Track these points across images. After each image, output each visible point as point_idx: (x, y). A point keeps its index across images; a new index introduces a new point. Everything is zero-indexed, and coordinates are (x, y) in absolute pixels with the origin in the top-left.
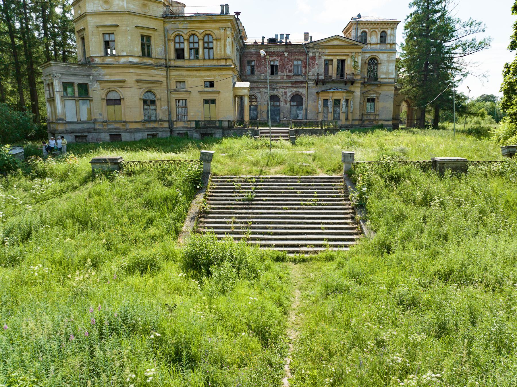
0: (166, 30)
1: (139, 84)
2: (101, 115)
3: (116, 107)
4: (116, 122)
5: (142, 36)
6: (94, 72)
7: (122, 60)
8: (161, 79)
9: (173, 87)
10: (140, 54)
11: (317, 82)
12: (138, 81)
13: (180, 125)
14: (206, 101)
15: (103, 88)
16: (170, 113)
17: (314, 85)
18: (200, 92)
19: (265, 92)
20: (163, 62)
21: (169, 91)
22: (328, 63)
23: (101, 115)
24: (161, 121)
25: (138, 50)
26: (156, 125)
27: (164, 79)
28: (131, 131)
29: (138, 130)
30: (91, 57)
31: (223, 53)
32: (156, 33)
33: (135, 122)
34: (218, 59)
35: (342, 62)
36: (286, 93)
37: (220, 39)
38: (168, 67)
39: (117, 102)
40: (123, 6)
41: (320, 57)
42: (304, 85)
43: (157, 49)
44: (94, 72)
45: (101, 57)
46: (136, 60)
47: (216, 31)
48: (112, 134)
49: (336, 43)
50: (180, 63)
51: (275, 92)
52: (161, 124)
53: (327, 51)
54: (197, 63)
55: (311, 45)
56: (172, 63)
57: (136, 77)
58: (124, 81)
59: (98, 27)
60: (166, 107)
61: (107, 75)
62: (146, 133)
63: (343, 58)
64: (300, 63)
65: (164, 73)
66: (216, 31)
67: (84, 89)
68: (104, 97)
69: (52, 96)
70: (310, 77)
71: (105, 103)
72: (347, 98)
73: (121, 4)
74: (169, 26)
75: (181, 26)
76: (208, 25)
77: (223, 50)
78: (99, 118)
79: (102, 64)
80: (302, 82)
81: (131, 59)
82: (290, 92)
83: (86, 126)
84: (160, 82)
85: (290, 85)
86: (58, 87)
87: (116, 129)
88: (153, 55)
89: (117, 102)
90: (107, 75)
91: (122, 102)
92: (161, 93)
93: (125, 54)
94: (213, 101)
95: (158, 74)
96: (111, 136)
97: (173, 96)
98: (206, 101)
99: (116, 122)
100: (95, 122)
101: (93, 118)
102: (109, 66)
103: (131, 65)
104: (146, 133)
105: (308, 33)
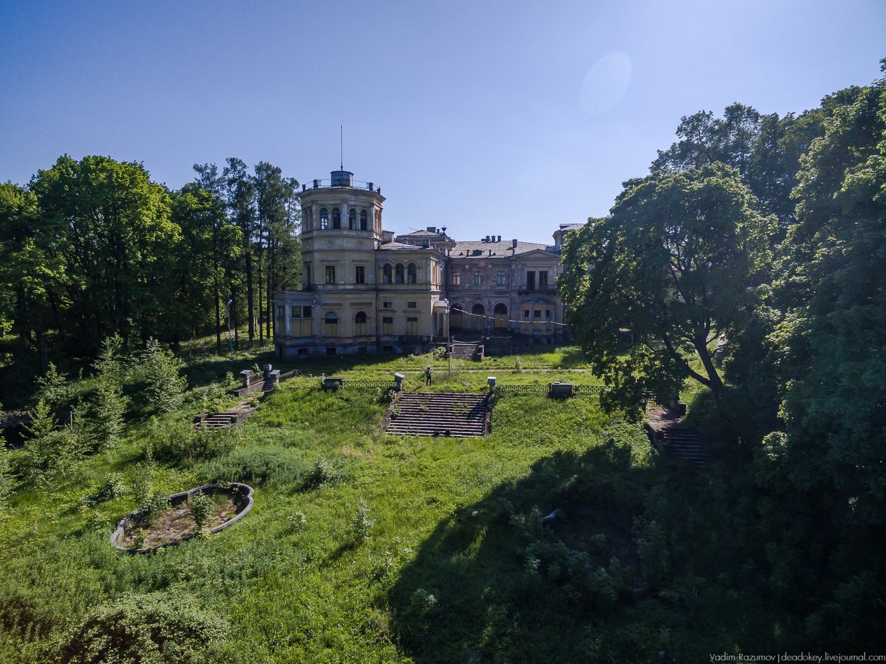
0: (377, 260)
1: (354, 307)
2: (320, 331)
3: (333, 324)
4: (332, 338)
5: (357, 268)
6: (316, 296)
7: (341, 287)
8: (371, 301)
9: (382, 307)
10: (355, 282)
11: (520, 293)
12: (352, 304)
13: (386, 339)
14: (409, 319)
15: (323, 309)
16: (377, 329)
17: (517, 295)
18: (404, 312)
19: (470, 302)
20: (374, 287)
21: (378, 311)
22: (531, 275)
23: (320, 331)
24: (370, 336)
25: (352, 278)
26: (365, 340)
27: (373, 301)
28: (345, 346)
29: (350, 345)
30: (315, 285)
31: (424, 279)
32: (369, 264)
33: (348, 338)
34: (420, 284)
35: (544, 275)
36: (489, 303)
37: (422, 267)
38: (377, 290)
39: (335, 321)
40: (343, 245)
41: (522, 269)
42: (507, 295)
43: (369, 277)
44: (317, 297)
45: (323, 285)
46: (351, 287)
47: (419, 261)
48: (330, 347)
49: (538, 255)
50: (387, 287)
51: (479, 302)
52: (370, 339)
53: (529, 263)
54: (402, 287)
55: (514, 258)
56: (381, 287)
57: (350, 301)
58: (340, 305)
59: (322, 261)
60: (374, 324)
61: (327, 299)
62: (357, 347)
63: (545, 269)
64: (503, 274)
65: (374, 296)
66: (419, 261)
67: (308, 312)
68: (323, 317)
69: (282, 315)
70: (513, 288)
71: (324, 321)
72: (548, 309)
73: (342, 244)
74: (379, 257)
75: (390, 257)
76: (412, 257)
77: (424, 277)
78: (318, 333)
79: (324, 291)
80: (505, 292)
81: (348, 287)
82: (495, 302)
83: (307, 341)
84: (370, 304)
85: (493, 295)
86: (288, 311)
87: (333, 343)
88: (365, 282)
89: (335, 321)
90: (327, 299)
91: (338, 321)
92: (370, 313)
93: (343, 283)
94: (415, 319)
95: (370, 297)
96: (328, 349)
97: (381, 314)
98: (409, 319)
99: (332, 338)
100: (314, 337)
101: (314, 334)
102: (330, 292)
103: (348, 291)
104: (357, 347)
105: (516, 240)
